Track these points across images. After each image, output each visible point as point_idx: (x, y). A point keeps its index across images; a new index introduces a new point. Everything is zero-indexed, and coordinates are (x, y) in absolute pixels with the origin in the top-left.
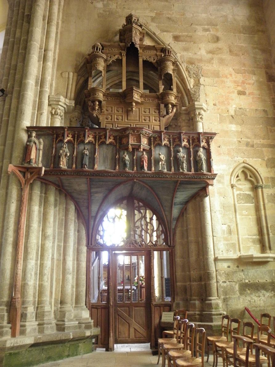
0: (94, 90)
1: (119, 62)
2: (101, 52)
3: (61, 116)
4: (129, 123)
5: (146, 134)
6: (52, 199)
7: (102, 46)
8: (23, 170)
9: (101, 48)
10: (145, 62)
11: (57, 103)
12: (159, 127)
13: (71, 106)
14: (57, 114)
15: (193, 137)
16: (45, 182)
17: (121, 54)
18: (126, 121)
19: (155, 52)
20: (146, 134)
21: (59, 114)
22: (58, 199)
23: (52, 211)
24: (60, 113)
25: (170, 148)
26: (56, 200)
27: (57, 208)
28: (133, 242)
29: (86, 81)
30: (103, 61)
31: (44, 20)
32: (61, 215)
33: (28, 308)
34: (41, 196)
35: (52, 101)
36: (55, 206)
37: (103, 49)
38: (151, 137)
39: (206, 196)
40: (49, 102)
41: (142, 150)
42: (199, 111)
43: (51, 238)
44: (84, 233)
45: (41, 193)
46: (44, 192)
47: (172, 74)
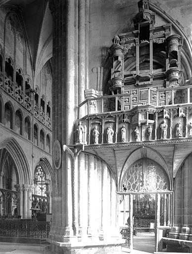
0: (115, 79)
1: (134, 48)
2: (120, 44)
7: (120, 37)
8: (73, 148)
9: (119, 40)
10: (155, 44)
12: (164, 102)
15: (189, 107)
16: (87, 154)
17: (134, 41)
19: (164, 32)
25: (170, 119)
29: (109, 74)
30: (120, 52)
31: (75, 26)
34: (85, 163)
35: (87, 94)
36: (95, 168)
37: (121, 41)
38: (155, 113)
41: (148, 124)
45: (85, 161)
47: (178, 51)
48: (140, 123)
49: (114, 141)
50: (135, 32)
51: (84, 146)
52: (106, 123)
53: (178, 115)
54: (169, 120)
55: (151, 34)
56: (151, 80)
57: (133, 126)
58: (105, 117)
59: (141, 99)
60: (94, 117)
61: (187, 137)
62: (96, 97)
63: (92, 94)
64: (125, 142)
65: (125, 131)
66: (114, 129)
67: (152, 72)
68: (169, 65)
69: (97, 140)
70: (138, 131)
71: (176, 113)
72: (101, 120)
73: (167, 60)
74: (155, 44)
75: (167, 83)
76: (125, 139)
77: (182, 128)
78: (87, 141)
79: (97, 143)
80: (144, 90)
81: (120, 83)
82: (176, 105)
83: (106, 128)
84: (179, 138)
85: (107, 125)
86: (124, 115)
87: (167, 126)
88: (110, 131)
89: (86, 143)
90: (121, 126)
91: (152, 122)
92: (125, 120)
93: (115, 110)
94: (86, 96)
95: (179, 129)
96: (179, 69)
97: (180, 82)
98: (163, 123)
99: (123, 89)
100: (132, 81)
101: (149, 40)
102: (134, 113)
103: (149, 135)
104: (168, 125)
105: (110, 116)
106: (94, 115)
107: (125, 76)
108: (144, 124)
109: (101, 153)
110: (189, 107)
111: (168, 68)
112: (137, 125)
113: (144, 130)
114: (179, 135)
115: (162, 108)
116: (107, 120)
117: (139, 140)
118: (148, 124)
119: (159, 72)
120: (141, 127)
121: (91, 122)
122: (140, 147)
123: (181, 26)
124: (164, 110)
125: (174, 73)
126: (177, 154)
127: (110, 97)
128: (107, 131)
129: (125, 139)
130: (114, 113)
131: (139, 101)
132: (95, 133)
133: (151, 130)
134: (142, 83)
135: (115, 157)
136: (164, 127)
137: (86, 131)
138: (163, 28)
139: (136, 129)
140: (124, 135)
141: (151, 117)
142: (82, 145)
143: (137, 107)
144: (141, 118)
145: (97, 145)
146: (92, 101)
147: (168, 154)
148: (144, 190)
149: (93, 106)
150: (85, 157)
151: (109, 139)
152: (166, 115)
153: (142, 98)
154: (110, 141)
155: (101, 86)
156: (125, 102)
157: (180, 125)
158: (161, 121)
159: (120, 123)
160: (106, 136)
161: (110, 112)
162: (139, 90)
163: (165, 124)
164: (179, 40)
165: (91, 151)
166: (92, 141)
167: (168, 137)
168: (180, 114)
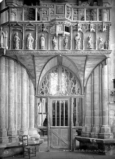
3: (15, 13)
4: (58, 16)
5: (67, 24)
6: (12, 68)
11: (11, 4)
12: (77, 18)
13: (20, 5)
14: (12, 12)
15: (98, 25)
18: (56, 14)
20: (67, 24)
21: (13, 12)
22: (16, 68)
23: (13, 75)
24: (14, 11)
25: (83, 33)
26: (15, 69)
27: (16, 74)
28: (61, 92)
32: (19, 78)
33: (3, 130)
35: (8, 2)
36: (15, 72)
39: (106, 64)
40: (6, 4)
41: (64, 35)
42: (105, 5)
43: (14, 91)
44: (33, 87)
45: (6, 65)
46: (7, 64)
48: (57, 34)
52: (26, 30)
53: (90, 30)
58: (25, 25)
59: (57, 13)
60: (15, 24)
61: (97, 49)
62: (17, 6)
63: (12, 2)
64: (44, 49)
65: (44, 40)
66: (34, 37)
69: (18, 45)
70: (55, 41)
71: (88, 29)
72: (22, 28)
76: (44, 46)
77: (93, 41)
79: (18, 49)
82: (88, 21)
83: (26, 35)
84: (91, 50)
85: (27, 33)
86: (43, 25)
87: (80, 39)
88: (31, 38)
89: (7, 48)
90: (40, 34)
93: (35, 20)
94: (7, 4)
95: (90, 42)
103: (66, 45)
104: (82, 39)
105: (30, 25)
106: (15, 22)
108: (61, 35)
109: (21, 58)
110: (98, 25)
112: (55, 35)
114: (90, 47)
115: (76, 22)
116: (27, 29)
117: (56, 48)
120: (59, 37)
121: (12, 28)
122: (57, 56)
124: (78, 25)
126: (88, 63)
127: (30, 7)
128: (27, 39)
129: (44, 46)
130: (34, 23)
132: (16, 39)
133: (67, 40)
135: (34, 63)
137: (7, 36)
139: (53, 38)
140: (43, 43)
141: (67, 29)
142: (4, 49)
145: (18, 50)
146: (13, 9)
147: (80, 63)
149: (14, 14)
150: (6, 61)
151: (29, 46)
152: (79, 29)
153: (59, 12)
154: (31, 48)
156: (43, 14)
157: (91, 39)
158: (75, 33)
161: (31, 21)
165: (11, 55)
166: (14, 47)
168: (91, 30)
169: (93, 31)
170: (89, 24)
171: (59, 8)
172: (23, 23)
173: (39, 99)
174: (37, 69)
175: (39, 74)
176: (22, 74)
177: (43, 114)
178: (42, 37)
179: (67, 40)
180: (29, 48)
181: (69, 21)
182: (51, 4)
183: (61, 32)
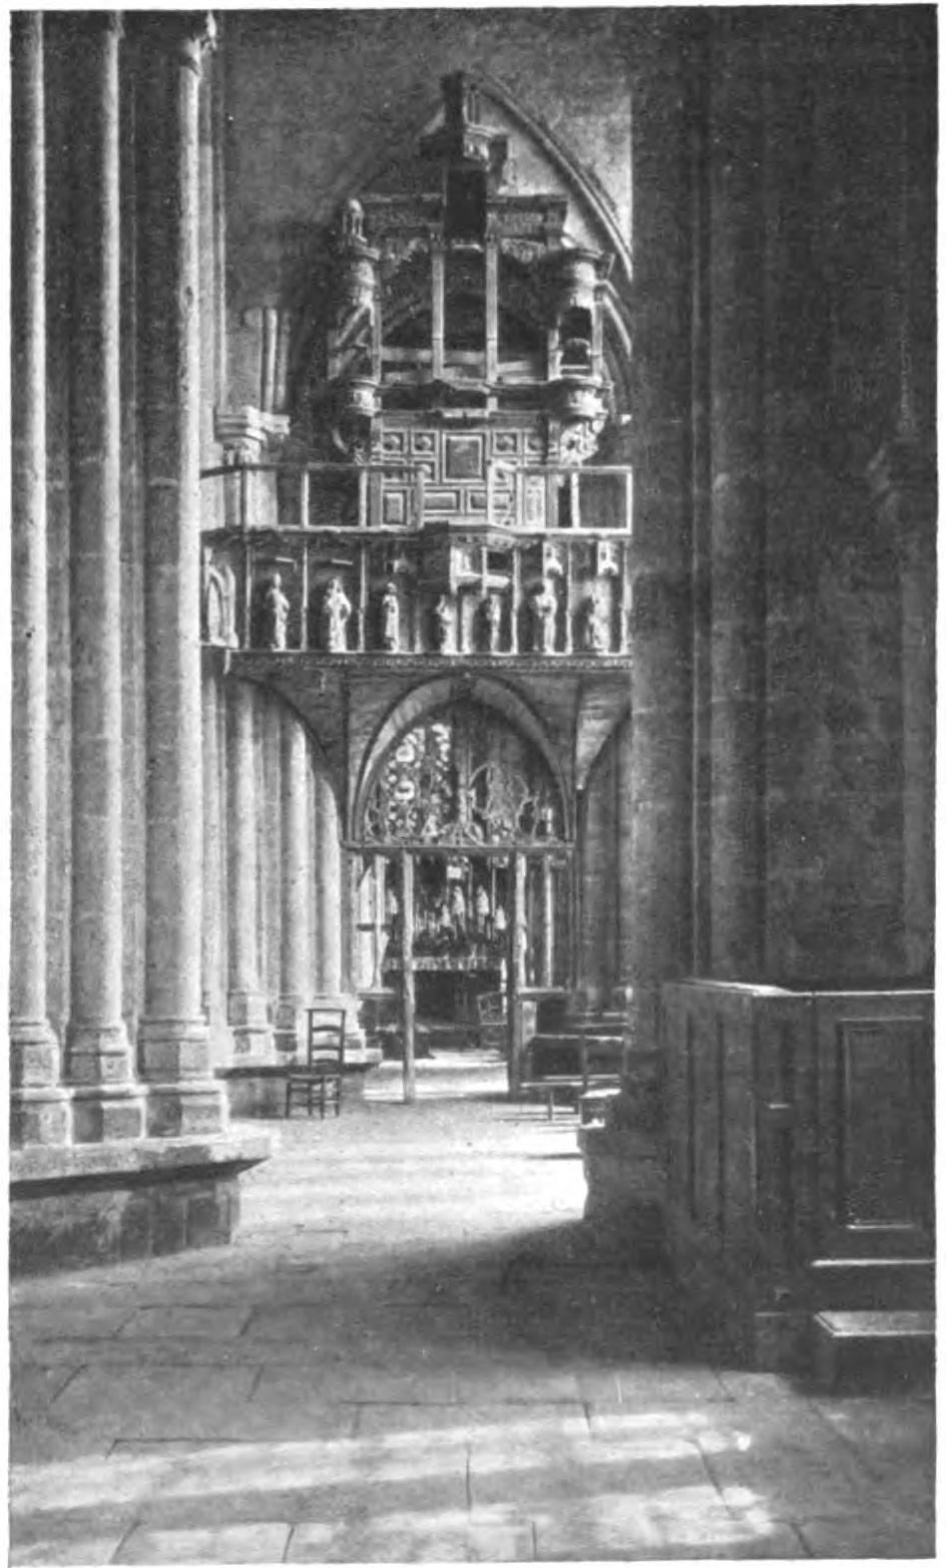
1: (422, 262)
19: (540, 218)
38: (510, 551)
44: (331, 805)
49: (352, 641)
50: (427, 197)
51: (228, 652)
54: (560, 583)
55: (492, 216)
56: (493, 404)
57: (427, 590)
66: (352, 591)
67: (500, 370)
68: (559, 355)
70: (448, 615)
71: (587, 563)
72: (296, 554)
73: (555, 338)
74: (508, 264)
75: (553, 426)
76: (396, 637)
78: (239, 628)
80: (464, 439)
81: (367, 400)
88: (338, 600)
89: (234, 642)
91: (500, 581)
92: (397, 564)
96: (596, 379)
97: (598, 426)
98: (539, 589)
99: (378, 425)
100: (417, 400)
101: (482, 242)
102: (429, 544)
107: (388, 367)
108: (470, 589)
111: (555, 374)
113: (468, 611)
116: (322, 558)
117: (449, 648)
118: (484, 592)
119: (515, 373)
121: (252, 556)
123: (606, 195)
125: (579, 394)
131: (445, 480)
133: (496, 615)
134: (458, 413)
136: (547, 610)
138: (536, 204)
143: (444, 528)
144: (459, 567)
148: (462, 839)
152: (551, 563)
154: (338, 644)
155: (282, 389)
159: (374, 572)
160: (319, 619)
162: (443, 436)
163: (547, 599)
164: (599, 265)
167: (560, 645)
169: (609, 574)
170: (590, 541)
171: (458, 450)
172: (306, 533)
173: (357, 861)
174: (354, 723)
175: (363, 746)
176: (285, 749)
177: (378, 930)
178: (387, 598)
179: (496, 615)
180: (332, 643)
181: (503, 531)
182: (420, 430)
183: (469, 575)
